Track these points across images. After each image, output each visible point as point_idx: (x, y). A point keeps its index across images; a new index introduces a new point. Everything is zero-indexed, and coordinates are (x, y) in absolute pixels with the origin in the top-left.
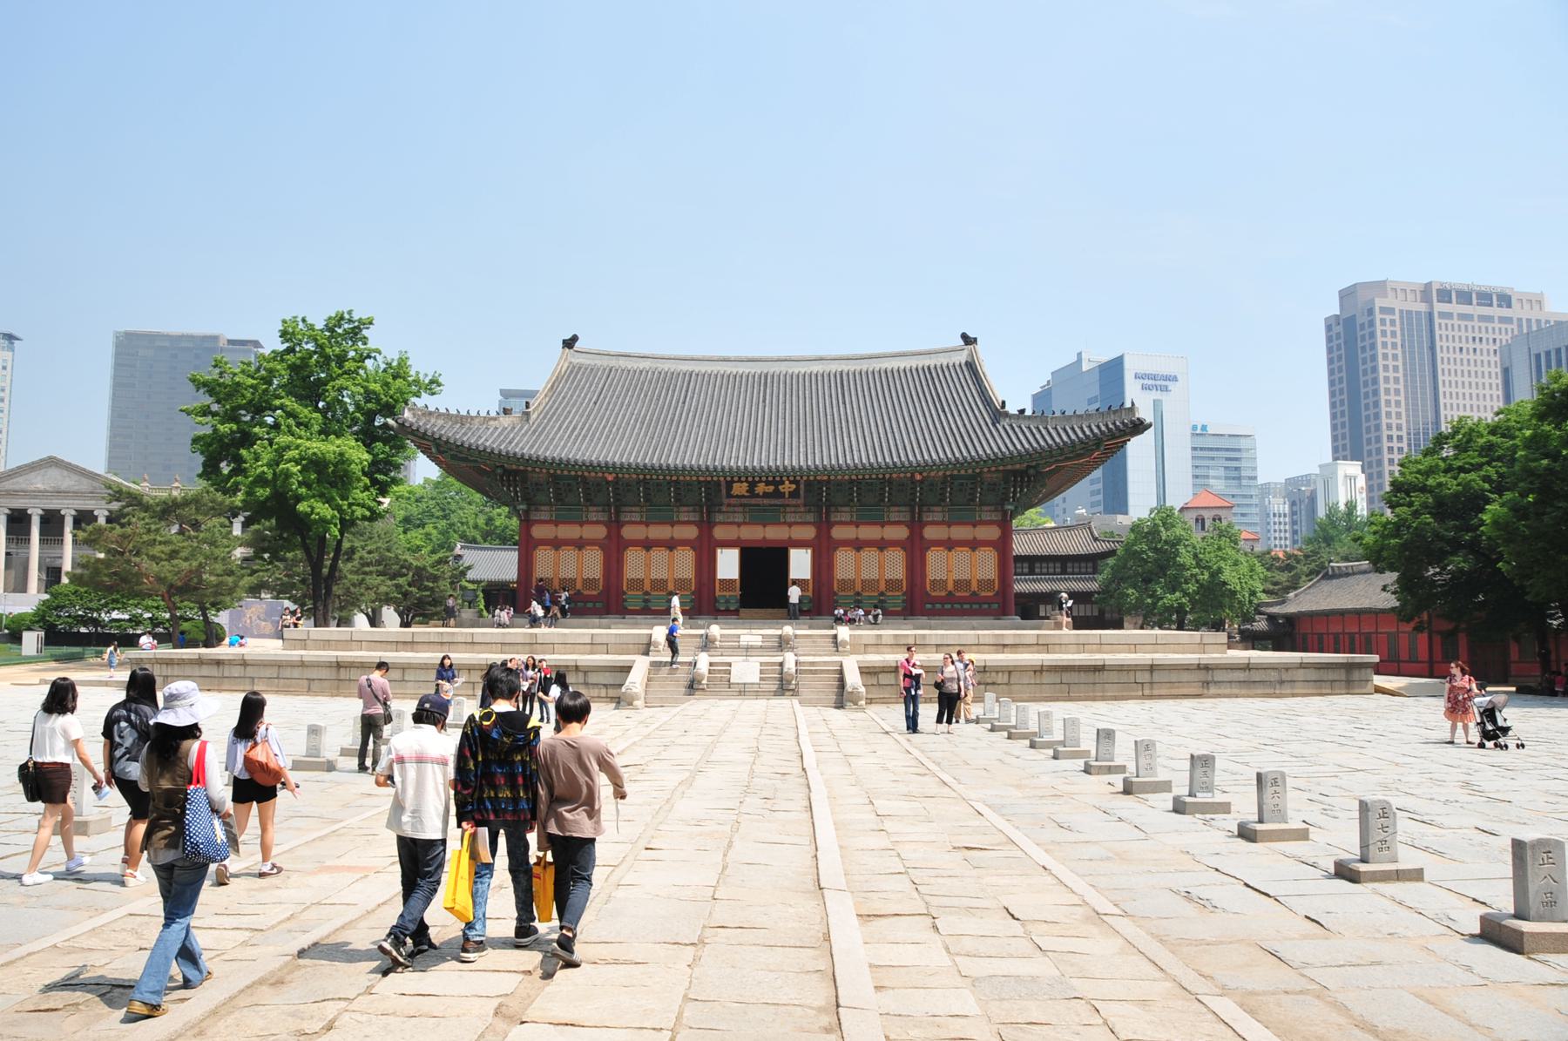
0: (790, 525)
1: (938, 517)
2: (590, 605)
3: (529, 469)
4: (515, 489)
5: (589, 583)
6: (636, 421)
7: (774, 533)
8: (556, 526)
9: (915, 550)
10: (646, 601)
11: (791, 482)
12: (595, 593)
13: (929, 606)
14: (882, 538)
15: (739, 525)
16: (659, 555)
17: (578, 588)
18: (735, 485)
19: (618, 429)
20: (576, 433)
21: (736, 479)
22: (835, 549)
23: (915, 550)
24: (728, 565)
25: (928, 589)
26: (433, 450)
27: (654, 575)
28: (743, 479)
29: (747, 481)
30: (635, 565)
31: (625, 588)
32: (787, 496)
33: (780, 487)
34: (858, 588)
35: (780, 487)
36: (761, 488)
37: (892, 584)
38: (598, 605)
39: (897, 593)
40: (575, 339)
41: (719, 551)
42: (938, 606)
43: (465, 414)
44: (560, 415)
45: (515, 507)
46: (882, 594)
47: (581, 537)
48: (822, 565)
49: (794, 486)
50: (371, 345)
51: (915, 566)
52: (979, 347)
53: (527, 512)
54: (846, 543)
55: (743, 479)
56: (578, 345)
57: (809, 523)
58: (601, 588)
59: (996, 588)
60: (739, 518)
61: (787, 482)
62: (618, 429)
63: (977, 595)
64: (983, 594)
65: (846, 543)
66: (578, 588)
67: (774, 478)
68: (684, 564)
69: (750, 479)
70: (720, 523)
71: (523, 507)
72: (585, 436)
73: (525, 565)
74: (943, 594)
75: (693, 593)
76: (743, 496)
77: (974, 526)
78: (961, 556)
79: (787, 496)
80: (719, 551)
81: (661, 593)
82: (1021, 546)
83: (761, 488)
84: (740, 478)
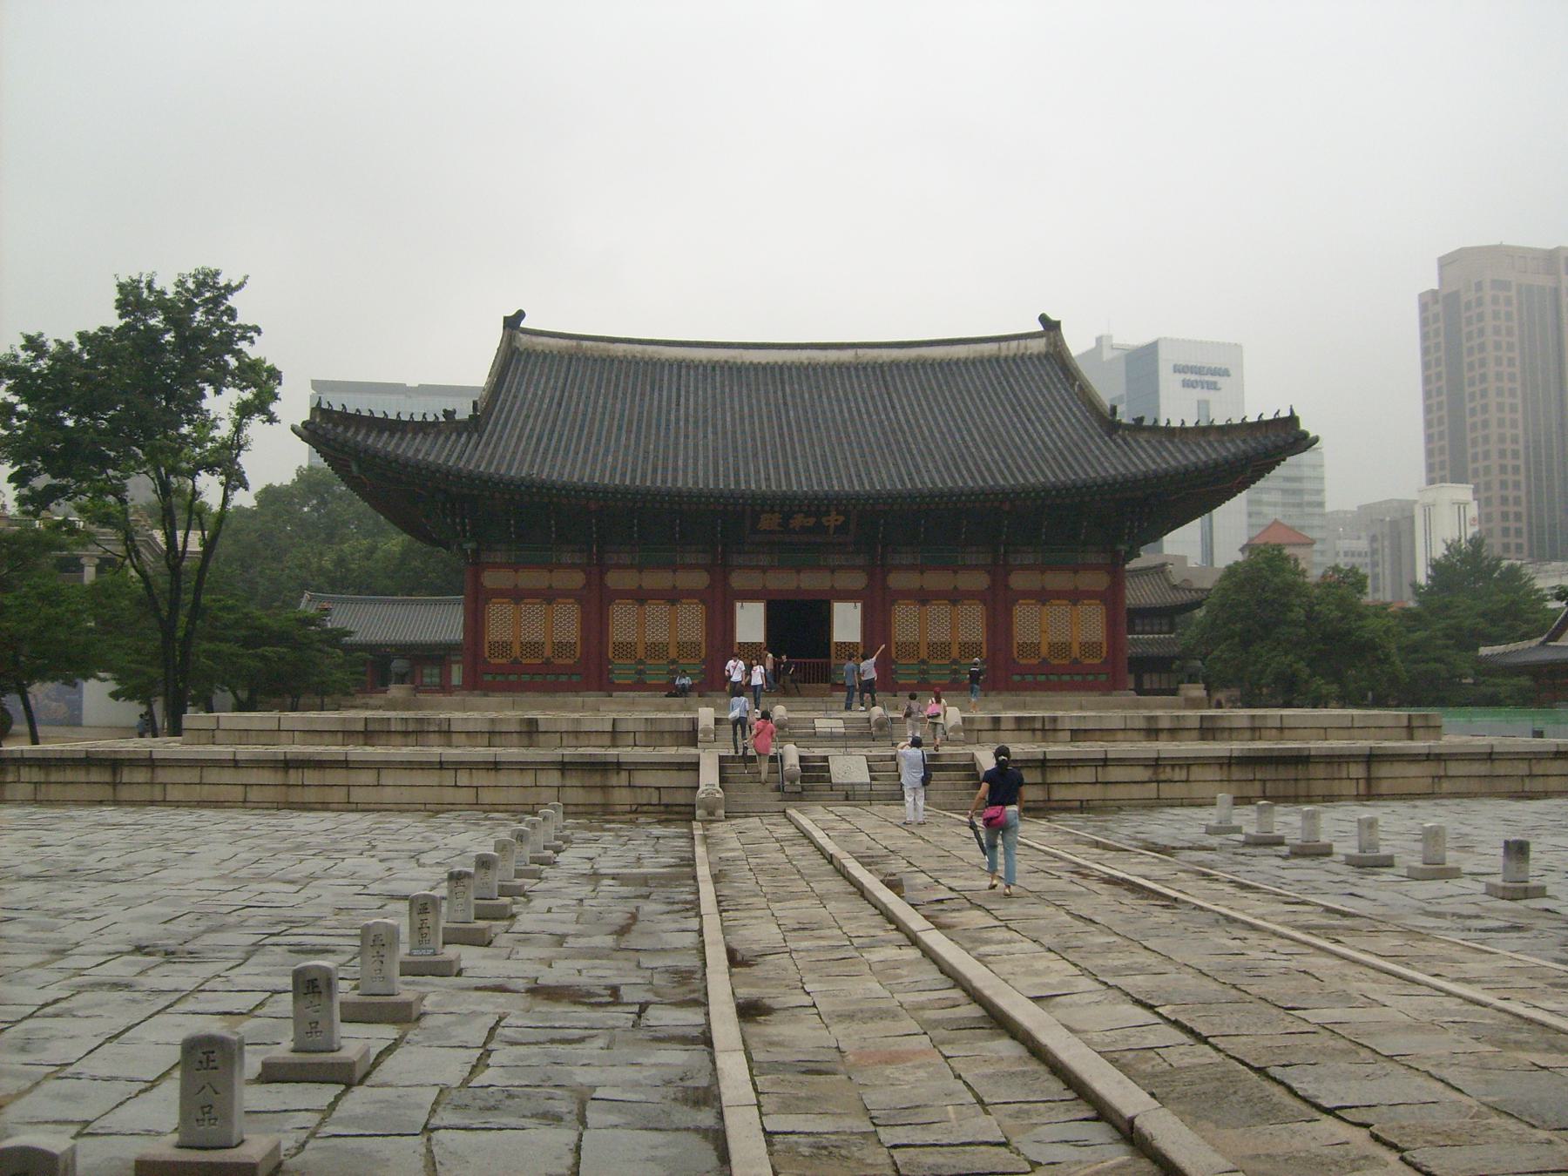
0: (833, 570)
1: (1029, 559)
2: (564, 678)
3: (487, 494)
4: (463, 525)
5: (561, 647)
6: (620, 428)
7: (811, 582)
8: (640, 572)
9: (999, 605)
10: (640, 672)
11: (838, 513)
13: (1016, 678)
15: (764, 570)
16: (657, 611)
17: (545, 655)
18: (763, 516)
19: (599, 440)
20: (543, 445)
21: (767, 508)
23: (999, 605)
24: (750, 622)
25: (1016, 655)
26: (354, 468)
27: (650, 638)
28: (777, 508)
29: (780, 512)
30: (624, 624)
31: (610, 655)
32: (831, 531)
33: (824, 520)
34: (924, 654)
35: (824, 520)
36: (798, 521)
37: (968, 649)
38: (575, 678)
40: (520, 315)
41: (738, 605)
42: (1029, 678)
43: (395, 418)
44: (516, 421)
45: (460, 545)
46: (955, 662)
47: (550, 587)
48: (875, 626)
49: (842, 518)
50: (241, 319)
51: (999, 626)
52: (1065, 330)
53: (476, 552)
54: (906, 595)
55: (777, 508)
56: (523, 324)
57: (860, 567)
58: (578, 655)
59: (1104, 654)
60: (764, 560)
61: (833, 513)
62: (599, 440)
63: (1081, 663)
65: (906, 595)
66: (545, 655)
67: (817, 506)
68: (690, 623)
69: (786, 509)
70: (740, 567)
71: (470, 546)
72: (557, 450)
73: (475, 623)
74: (1035, 661)
75: (704, 662)
76: (772, 532)
77: (1076, 572)
78: (1059, 611)
79: (831, 531)
80: (738, 605)
82: (1138, 594)
83: (798, 521)
84: (772, 507)
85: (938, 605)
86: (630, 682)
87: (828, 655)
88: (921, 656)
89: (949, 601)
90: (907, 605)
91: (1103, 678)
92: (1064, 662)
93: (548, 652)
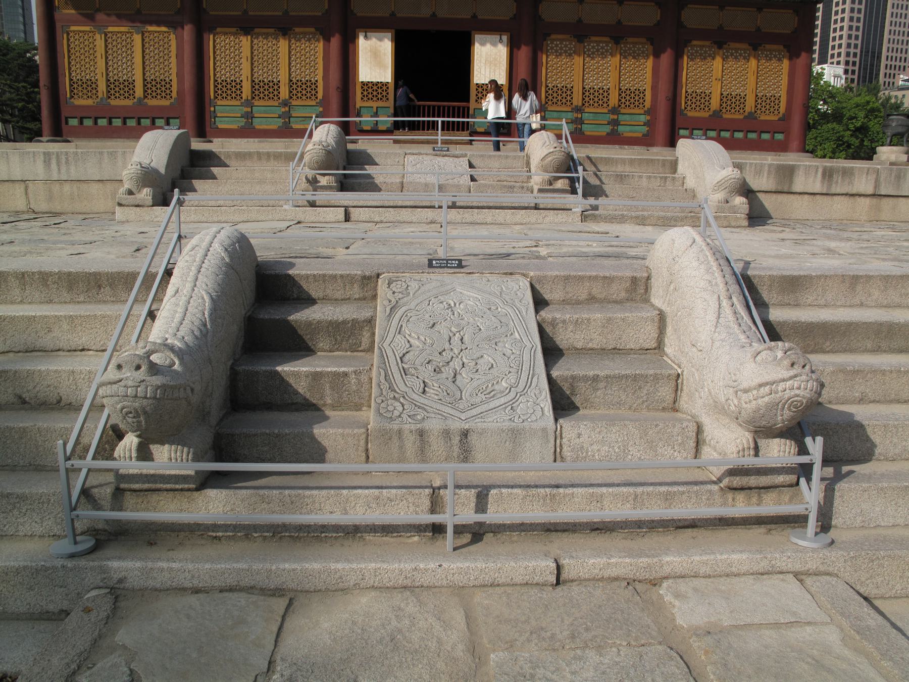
12: (165, 103)
14: (619, 22)
22: (546, 36)
37: (630, 98)
39: (637, 111)
58: (174, 95)
59: (782, 110)
63: (756, 118)
64: (763, 117)
75: (320, 104)
81: (271, 103)
85: (598, 42)
86: (234, 126)
87: (468, 101)
88: (575, 103)
89: (611, 37)
90: (561, 41)
91: (779, 137)
92: (737, 116)
93: (139, 92)
